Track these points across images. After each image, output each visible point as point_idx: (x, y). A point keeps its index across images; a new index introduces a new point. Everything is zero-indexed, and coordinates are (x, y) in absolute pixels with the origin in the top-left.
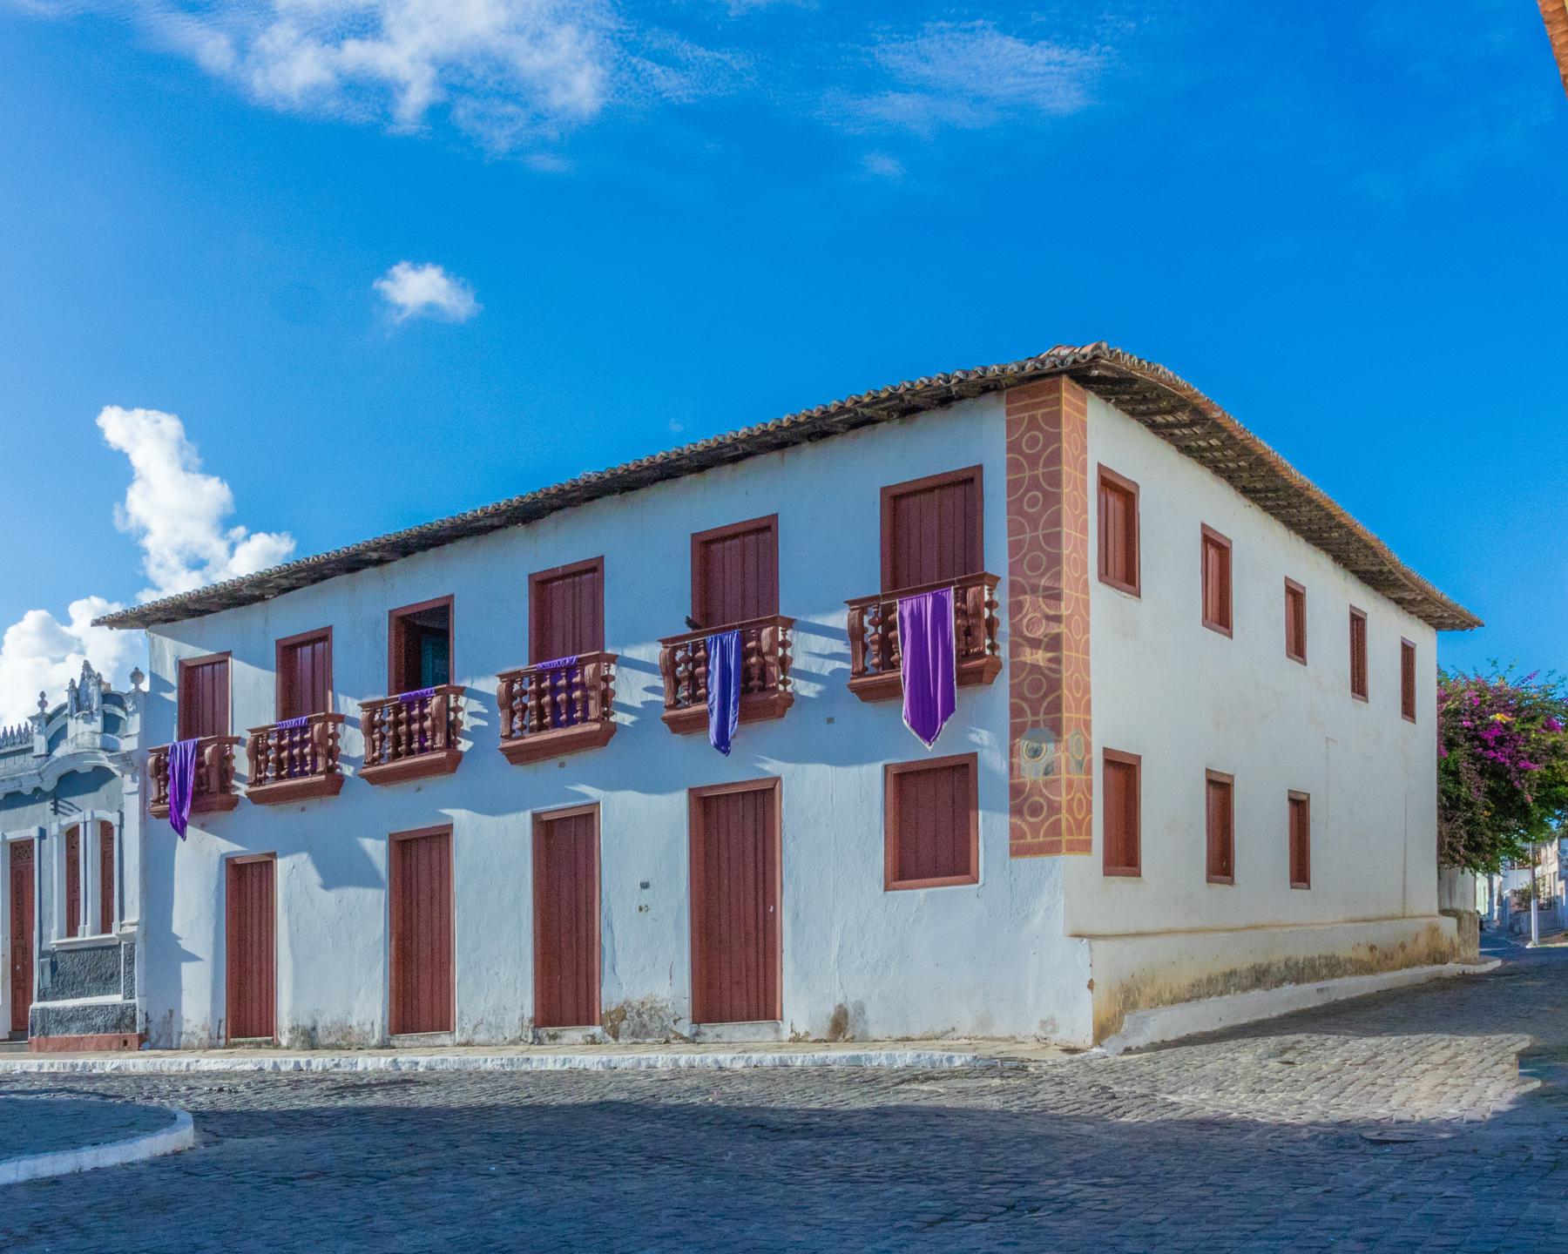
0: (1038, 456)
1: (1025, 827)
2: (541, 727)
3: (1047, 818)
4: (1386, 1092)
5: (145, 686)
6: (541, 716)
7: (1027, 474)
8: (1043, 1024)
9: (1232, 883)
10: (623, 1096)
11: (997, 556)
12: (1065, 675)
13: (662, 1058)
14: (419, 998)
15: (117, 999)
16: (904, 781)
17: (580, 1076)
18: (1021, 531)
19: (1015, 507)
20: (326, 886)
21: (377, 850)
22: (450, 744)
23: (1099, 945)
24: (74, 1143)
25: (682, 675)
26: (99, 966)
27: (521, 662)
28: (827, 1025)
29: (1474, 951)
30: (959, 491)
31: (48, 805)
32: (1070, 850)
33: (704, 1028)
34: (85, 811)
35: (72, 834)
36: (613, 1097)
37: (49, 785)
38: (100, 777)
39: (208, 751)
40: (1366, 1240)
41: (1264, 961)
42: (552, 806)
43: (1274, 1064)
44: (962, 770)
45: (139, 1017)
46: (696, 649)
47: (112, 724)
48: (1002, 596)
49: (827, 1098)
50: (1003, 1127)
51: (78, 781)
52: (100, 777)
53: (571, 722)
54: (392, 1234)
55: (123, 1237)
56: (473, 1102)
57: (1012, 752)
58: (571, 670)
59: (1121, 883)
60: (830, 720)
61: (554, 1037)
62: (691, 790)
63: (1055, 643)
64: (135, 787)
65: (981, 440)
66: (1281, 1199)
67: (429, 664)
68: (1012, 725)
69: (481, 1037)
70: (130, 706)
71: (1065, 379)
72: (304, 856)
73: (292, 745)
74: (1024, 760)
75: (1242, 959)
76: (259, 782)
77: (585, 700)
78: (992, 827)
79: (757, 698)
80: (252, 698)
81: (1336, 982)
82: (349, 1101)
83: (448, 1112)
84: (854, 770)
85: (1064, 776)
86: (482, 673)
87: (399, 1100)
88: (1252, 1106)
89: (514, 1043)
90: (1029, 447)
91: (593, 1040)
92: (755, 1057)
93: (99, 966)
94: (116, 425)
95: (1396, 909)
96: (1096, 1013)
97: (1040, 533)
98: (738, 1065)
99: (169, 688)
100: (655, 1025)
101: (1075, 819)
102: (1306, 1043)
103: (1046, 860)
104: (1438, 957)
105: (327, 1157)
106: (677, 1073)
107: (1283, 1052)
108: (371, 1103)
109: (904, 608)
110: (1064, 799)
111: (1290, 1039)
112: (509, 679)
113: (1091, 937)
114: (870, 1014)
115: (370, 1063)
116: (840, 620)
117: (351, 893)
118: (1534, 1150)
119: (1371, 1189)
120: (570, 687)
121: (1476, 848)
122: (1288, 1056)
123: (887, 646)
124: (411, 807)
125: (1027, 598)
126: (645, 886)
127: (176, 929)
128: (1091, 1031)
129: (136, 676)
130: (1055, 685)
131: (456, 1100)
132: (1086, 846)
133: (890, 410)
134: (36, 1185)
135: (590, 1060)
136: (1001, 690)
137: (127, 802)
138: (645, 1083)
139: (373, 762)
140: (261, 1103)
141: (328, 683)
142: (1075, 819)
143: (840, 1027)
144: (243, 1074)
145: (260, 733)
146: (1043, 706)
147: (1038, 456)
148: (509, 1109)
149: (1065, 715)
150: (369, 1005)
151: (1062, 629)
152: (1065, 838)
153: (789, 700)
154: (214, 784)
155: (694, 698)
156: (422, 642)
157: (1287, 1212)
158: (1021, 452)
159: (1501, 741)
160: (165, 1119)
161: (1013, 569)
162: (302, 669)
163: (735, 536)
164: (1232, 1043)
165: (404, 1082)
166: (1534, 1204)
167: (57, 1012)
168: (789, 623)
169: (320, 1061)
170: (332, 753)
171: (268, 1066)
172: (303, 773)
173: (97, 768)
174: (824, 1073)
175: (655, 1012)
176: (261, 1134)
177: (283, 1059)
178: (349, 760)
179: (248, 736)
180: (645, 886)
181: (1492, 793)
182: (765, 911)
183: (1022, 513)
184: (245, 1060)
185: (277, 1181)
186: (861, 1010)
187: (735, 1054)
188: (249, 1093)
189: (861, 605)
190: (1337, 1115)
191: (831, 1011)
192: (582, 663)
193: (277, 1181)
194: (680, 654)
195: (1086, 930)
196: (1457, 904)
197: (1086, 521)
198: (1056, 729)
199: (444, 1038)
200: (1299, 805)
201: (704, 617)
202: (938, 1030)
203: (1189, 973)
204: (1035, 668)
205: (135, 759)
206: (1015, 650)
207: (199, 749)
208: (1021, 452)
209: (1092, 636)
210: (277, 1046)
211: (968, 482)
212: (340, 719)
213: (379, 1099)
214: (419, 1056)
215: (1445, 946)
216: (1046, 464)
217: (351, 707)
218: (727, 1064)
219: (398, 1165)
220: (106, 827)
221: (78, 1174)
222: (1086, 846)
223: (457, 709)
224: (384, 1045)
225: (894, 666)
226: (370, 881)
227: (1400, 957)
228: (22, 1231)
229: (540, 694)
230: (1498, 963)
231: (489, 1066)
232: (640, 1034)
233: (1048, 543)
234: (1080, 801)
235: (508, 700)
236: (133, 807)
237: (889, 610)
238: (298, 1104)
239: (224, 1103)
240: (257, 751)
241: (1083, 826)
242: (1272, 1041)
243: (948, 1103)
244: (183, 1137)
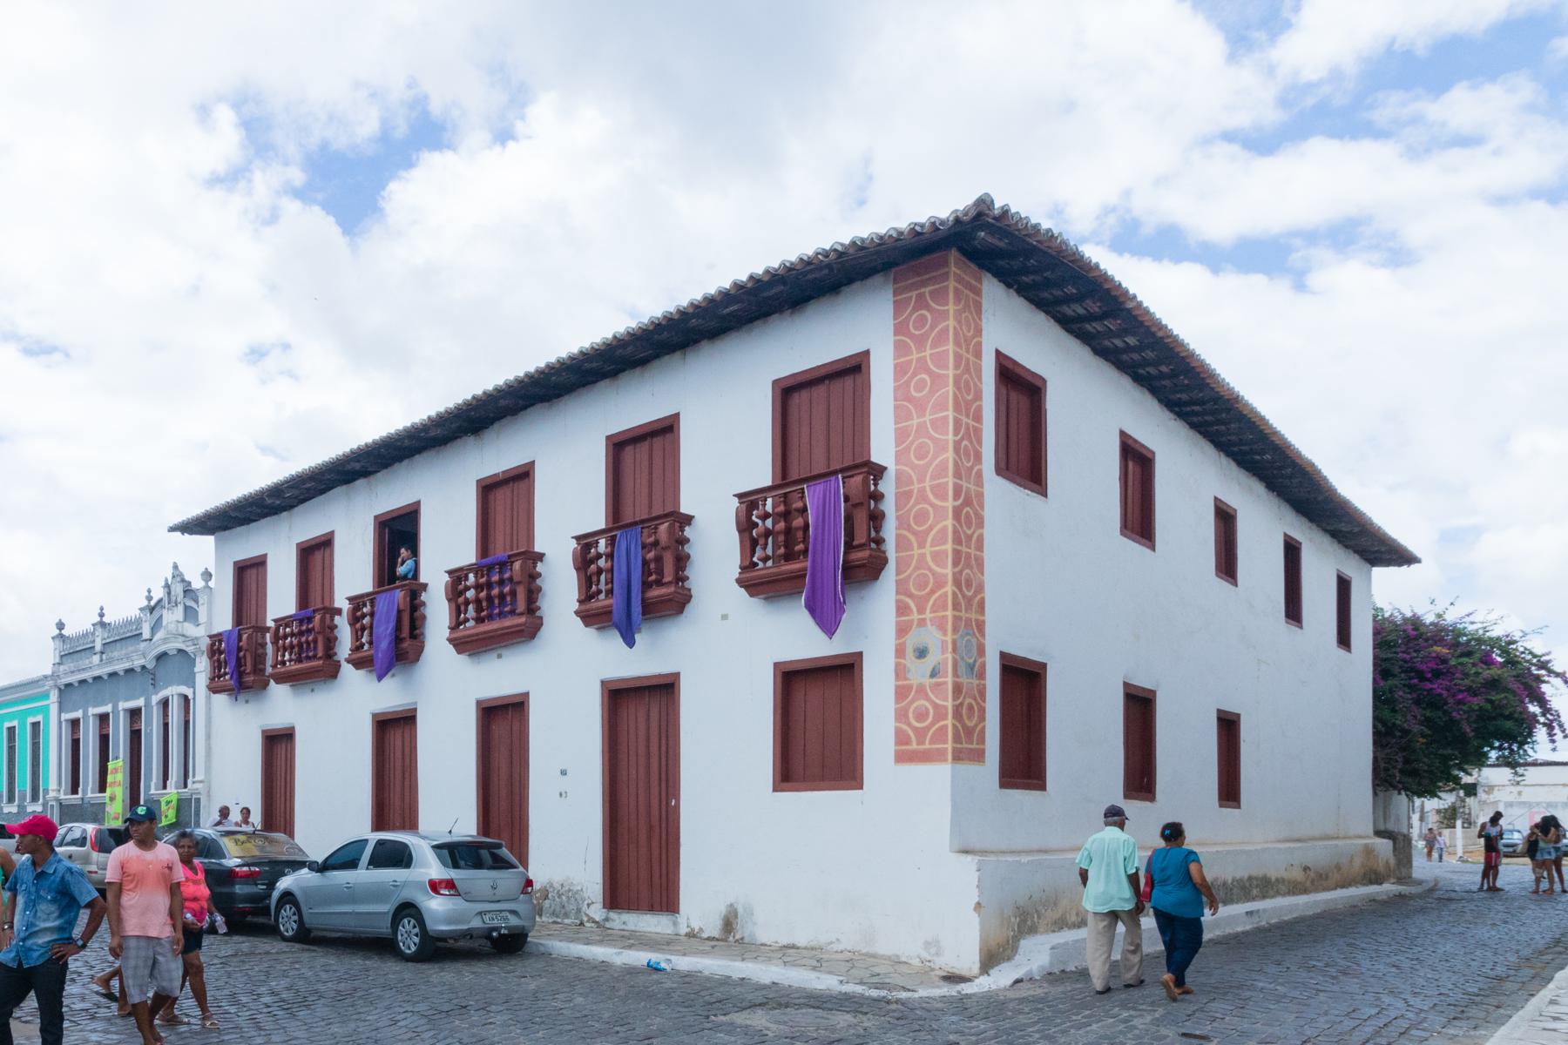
8: (927, 945)
19: (902, 393)
28: (719, 923)
44: (846, 670)
59: (1021, 798)
68: (898, 623)
71: (953, 255)
90: (916, 328)
96: (984, 940)
97: (928, 418)
101: (964, 726)
104: (1374, 878)
113: (984, 852)
121: (1414, 773)
126: (564, 773)
128: (977, 958)
132: (978, 756)
142: (964, 726)
159: (1438, 674)
181: (1428, 722)
182: (668, 804)
183: (909, 399)
195: (978, 846)
197: (979, 411)
211: (854, 369)
215: (1381, 868)
222: (978, 756)
233: (935, 430)
234: (970, 708)
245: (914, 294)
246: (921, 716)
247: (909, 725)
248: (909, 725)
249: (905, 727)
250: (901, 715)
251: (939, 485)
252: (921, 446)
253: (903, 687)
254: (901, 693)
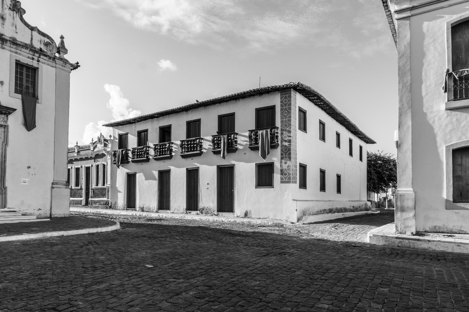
2: (188, 151)
4: (356, 236)
5: (112, 138)
6: (188, 149)
9: (325, 192)
10: (203, 225)
11: (278, 123)
12: (292, 148)
13: (211, 219)
14: (164, 202)
15: (105, 199)
16: (260, 167)
17: (195, 221)
18: (283, 118)
19: (282, 114)
20: (146, 180)
21: (156, 174)
22: (170, 154)
23: (298, 202)
24: (97, 227)
25: (216, 142)
26: (102, 192)
27: (184, 138)
29: (374, 209)
30: (271, 110)
31: (93, 160)
32: (292, 183)
33: (219, 213)
34: (100, 162)
35: (98, 166)
36: (201, 225)
37: (93, 157)
38: (103, 155)
39: (124, 152)
40: (352, 266)
41: (331, 208)
42: (190, 167)
43: (333, 229)
44: (271, 166)
45: (110, 203)
46: (219, 138)
47: (105, 145)
48: (279, 131)
49: (243, 229)
50: (278, 237)
51: (99, 156)
52: (103, 155)
53: (194, 151)
54: (158, 249)
55: (106, 246)
56: (174, 224)
57: (281, 162)
58: (194, 140)
60: (245, 154)
61: (190, 213)
62: (217, 166)
63: (290, 141)
64: (110, 158)
65: (275, 100)
66: (335, 256)
67: (167, 138)
69: (175, 212)
70: (109, 142)
72: (142, 173)
73: (140, 152)
74: (283, 164)
75: (327, 207)
76: (133, 158)
77: (197, 146)
78: (277, 177)
79: (230, 148)
80: (132, 142)
81: (346, 213)
82: (150, 222)
83: (169, 226)
84: (249, 164)
85: (291, 168)
86: (177, 140)
87: (159, 223)
88: (329, 237)
89: (182, 213)
91: (197, 214)
92: (229, 220)
93: (102, 192)
94: (108, 88)
95: (358, 199)
96: (298, 216)
98: (226, 221)
99: (117, 139)
100: (210, 212)
102: (340, 225)
103: (288, 184)
105: (145, 233)
106: (214, 222)
107: (335, 226)
108: (154, 223)
109: (260, 132)
110: (291, 172)
111: (337, 224)
112: (182, 141)
113: (296, 200)
114: (252, 213)
115: (154, 215)
116: (247, 134)
117: (151, 181)
118: (387, 250)
119: (353, 256)
120: (194, 144)
122: (336, 227)
123: (256, 140)
124: (163, 165)
125: (284, 132)
127: (117, 186)
129: (110, 136)
130: (290, 150)
131: (171, 224)
132: (296, 182)
133: (257, 93)
134: (89, 234)
135: (197, 218)
136: (278, 151)
137: (108, 160)
138: (208, 223)
139: (155, 156)
140: (133, 221)
141: (147, 140)
143: (246, 215)
144: (129, 216)
145: (134, 149)
146: (287, 153)
147: (286, 104)
148: (181, 226)
149: (292, 156)
150: (154, 204)
151: (291, 138)
152: (291, 180)
153: (237, 149)
154: (125, 158)
155: (218, 148)
156: (165, 133)
157: (336, 259)
160: (114, 223)
161: (282, 126)
162: (142, 137)
163: (226, 116)
164: (325, 224)
165: (160, 220)
166: (387, 261)
167: (94, 201)
168: (237, 134)
169: (144, 214)
170: (148, 154)
171: (134, 215)
172: (142, 157)
173: (103, 154)
174: (243, 224)
175: (210, 209)
176: (133, 227)
177: (137, 213)
178: (151, 155)
179: (132, 150)
180: (208, 184)
183: (284, 115)
184: (130, 213)
185: (136, 237)
186: (250, 212)
187: (225, 219)
188: (130, 219)
189: (251, 131)
190: (346, 240)
191: (245, 212)
192: (196, 139)
193: (136, 237)
194: (215, 139)
195: (296, 199)
196: (371, 199)
198: (290, 158)
199: (168, 211)
200: (339, 177)
201: (220, 132)
202: (266, 217)
203: (316, 209)
204: (286, 146)
205: (110, 152)
206: (282, 142)
207: (122, 151)
209: (297, 140)
210: (136, 211)
211: (273, 108)
212: (149, 147)
213: (155, 222)
214: (163, 214)
217: (151, 145)
218: (224, 221)
219: (159, 236)
220: (104, 165)
221: (98, 233)
222: (296, 182)
223: (172, 147)
224: (157, 212)
225: (258, 144)
226: (154, 179)
227: (359, 209)
228: (87, 243)
229: (188, 145)
230: (379, 212)
231: (177, 218)
232: (207, 213)
235: (182, 146)
236: (109, 162)
237: (257, 132)
238: (140, 222)
239: (126, 221)
240: (133, 152)
241: (295, 178)
242: (333, 224)
243: (268, 232)
244: (117, 227)
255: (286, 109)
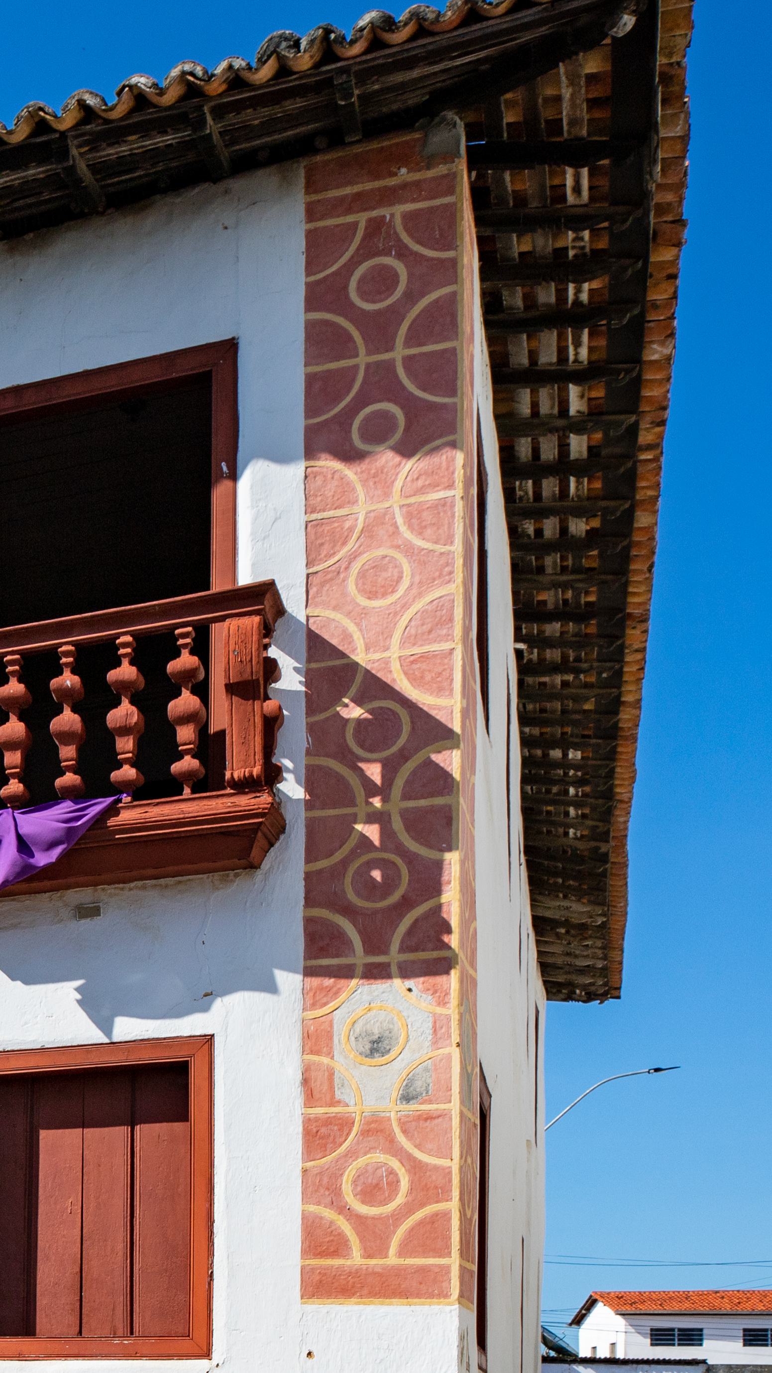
0: (395, 314)
1: (346, 1227)
3: (409, 1209)
7: (363, 359)
74: (344, 1060)
90: (364, 295)
158: (346, 309)
208: (346, 309)
216: (413, 339)
233: (420, 531)
245: (362, 218)
246: (372, 1191)
247: (343, 1210)
248: (343, 1210)
249: (328, 1214)
250: (319, 1186)
251: (424, 657)
252: (378, 566)
253: (328, 1121)
254: (319, 1136)
255: (383, 382)
